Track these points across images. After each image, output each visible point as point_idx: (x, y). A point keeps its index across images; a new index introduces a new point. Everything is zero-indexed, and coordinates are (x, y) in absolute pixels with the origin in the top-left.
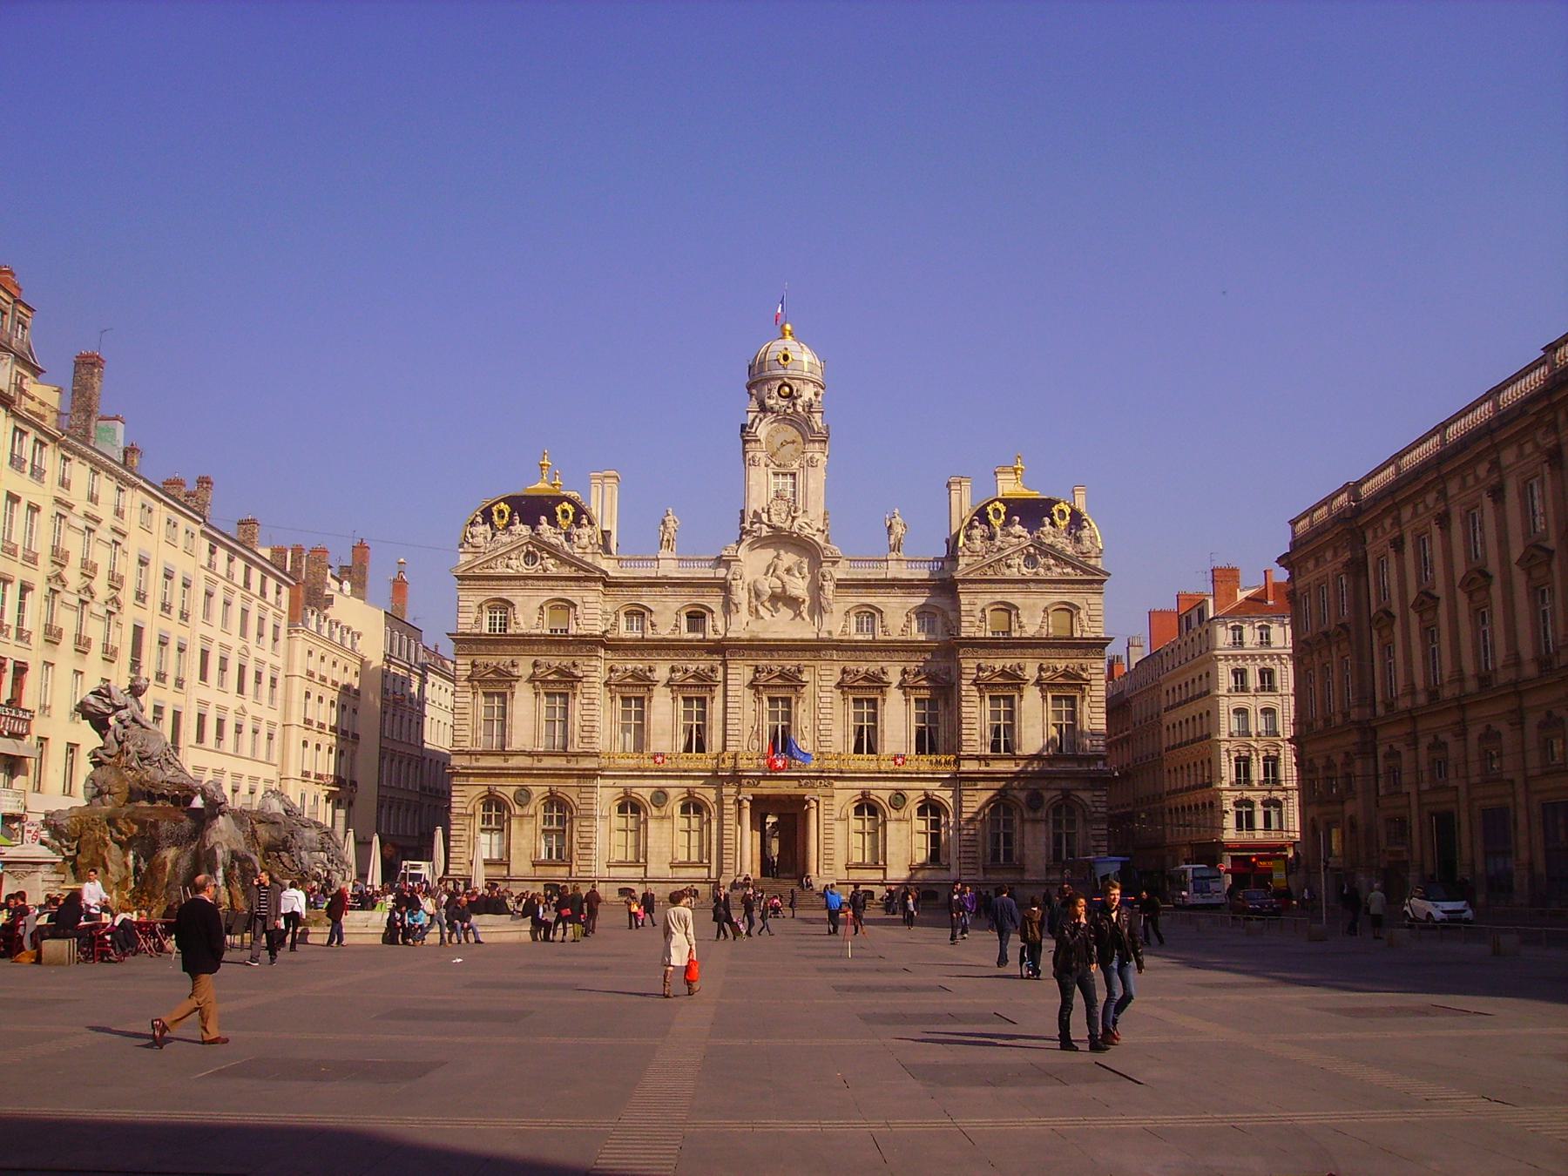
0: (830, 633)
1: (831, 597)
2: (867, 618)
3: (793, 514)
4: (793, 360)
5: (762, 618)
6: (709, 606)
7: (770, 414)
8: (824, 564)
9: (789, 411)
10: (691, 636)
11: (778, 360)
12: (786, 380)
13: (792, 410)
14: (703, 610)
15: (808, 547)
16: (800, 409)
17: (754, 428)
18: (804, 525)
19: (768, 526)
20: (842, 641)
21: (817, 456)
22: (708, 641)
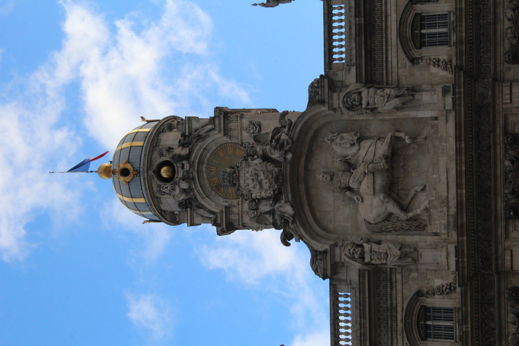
0: (445, 91)
1: (387, 91)
2: (422, 27)
3: (258, 161)
4: (128, 162)
5: (427, 209)
6: (409, 299)
7: (192, 193)
8: (335, 106)
9: (187, 166)
10: (457, 333)
11: (129, 182)
12: (151, 172)
13: (185, 162)
14: (416, 311)
15: (311, 133)
16: (185, 152)
17: (212, 216)
18: (273, 143)
19: (276, 198)
20: (459, 68)
21: (245, 122)
22: (464, 302)
